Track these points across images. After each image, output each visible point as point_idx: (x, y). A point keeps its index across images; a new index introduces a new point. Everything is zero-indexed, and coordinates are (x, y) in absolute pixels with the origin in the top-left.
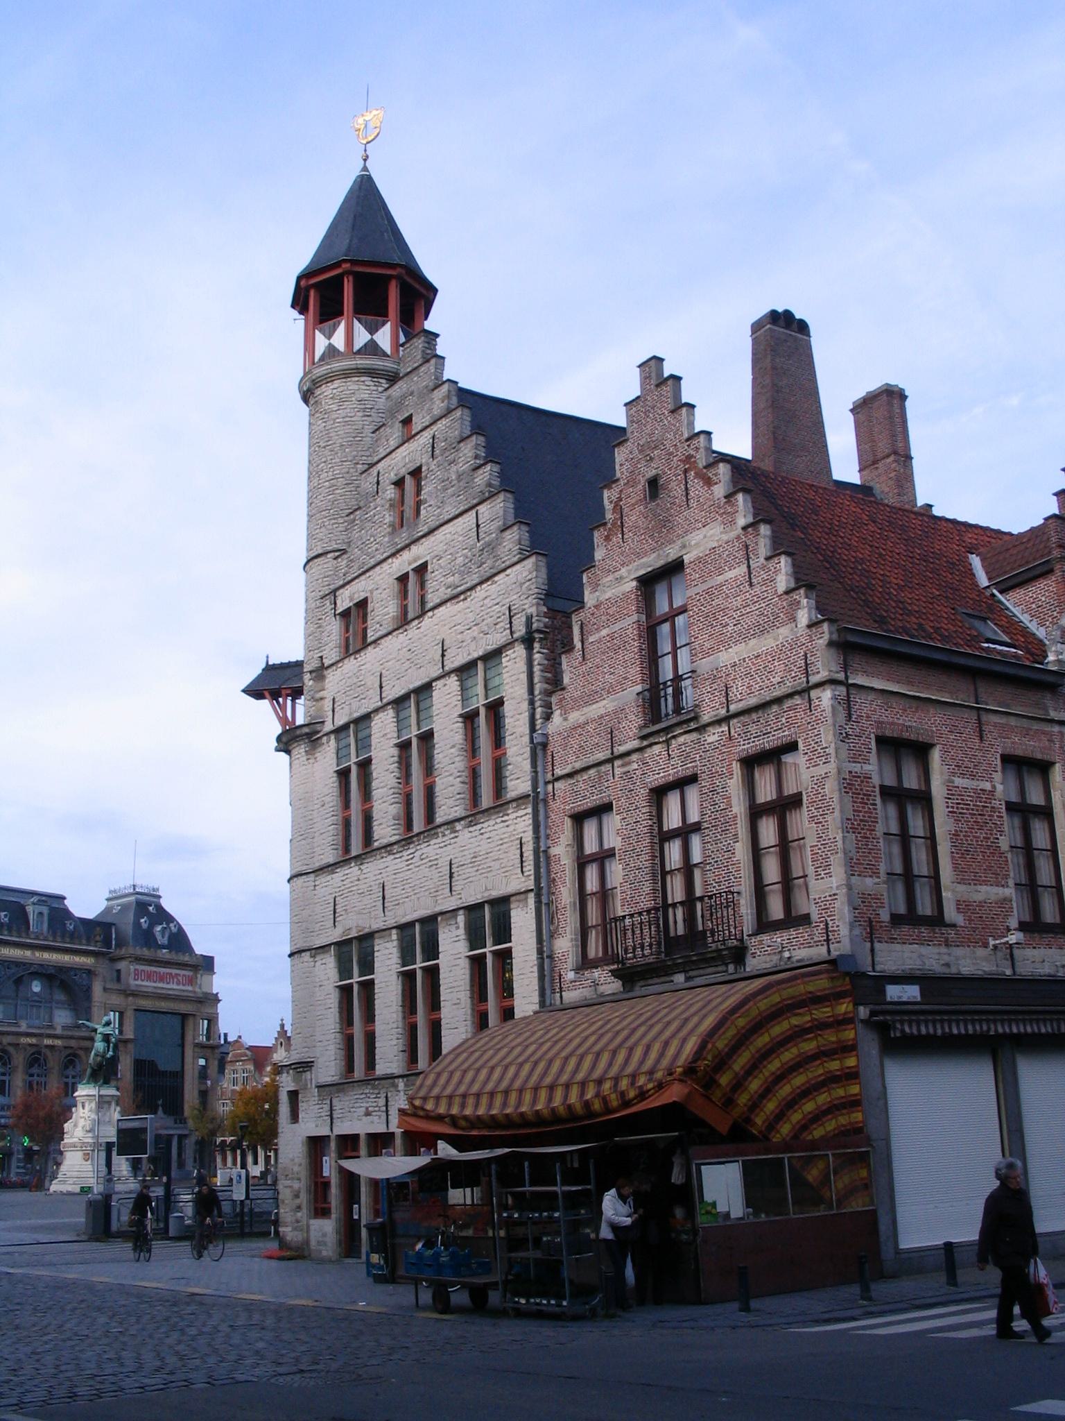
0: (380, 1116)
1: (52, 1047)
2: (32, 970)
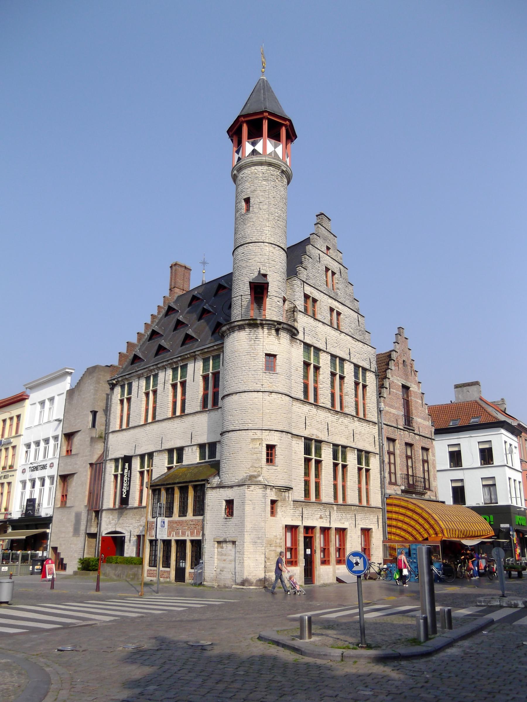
0: (326, 520)
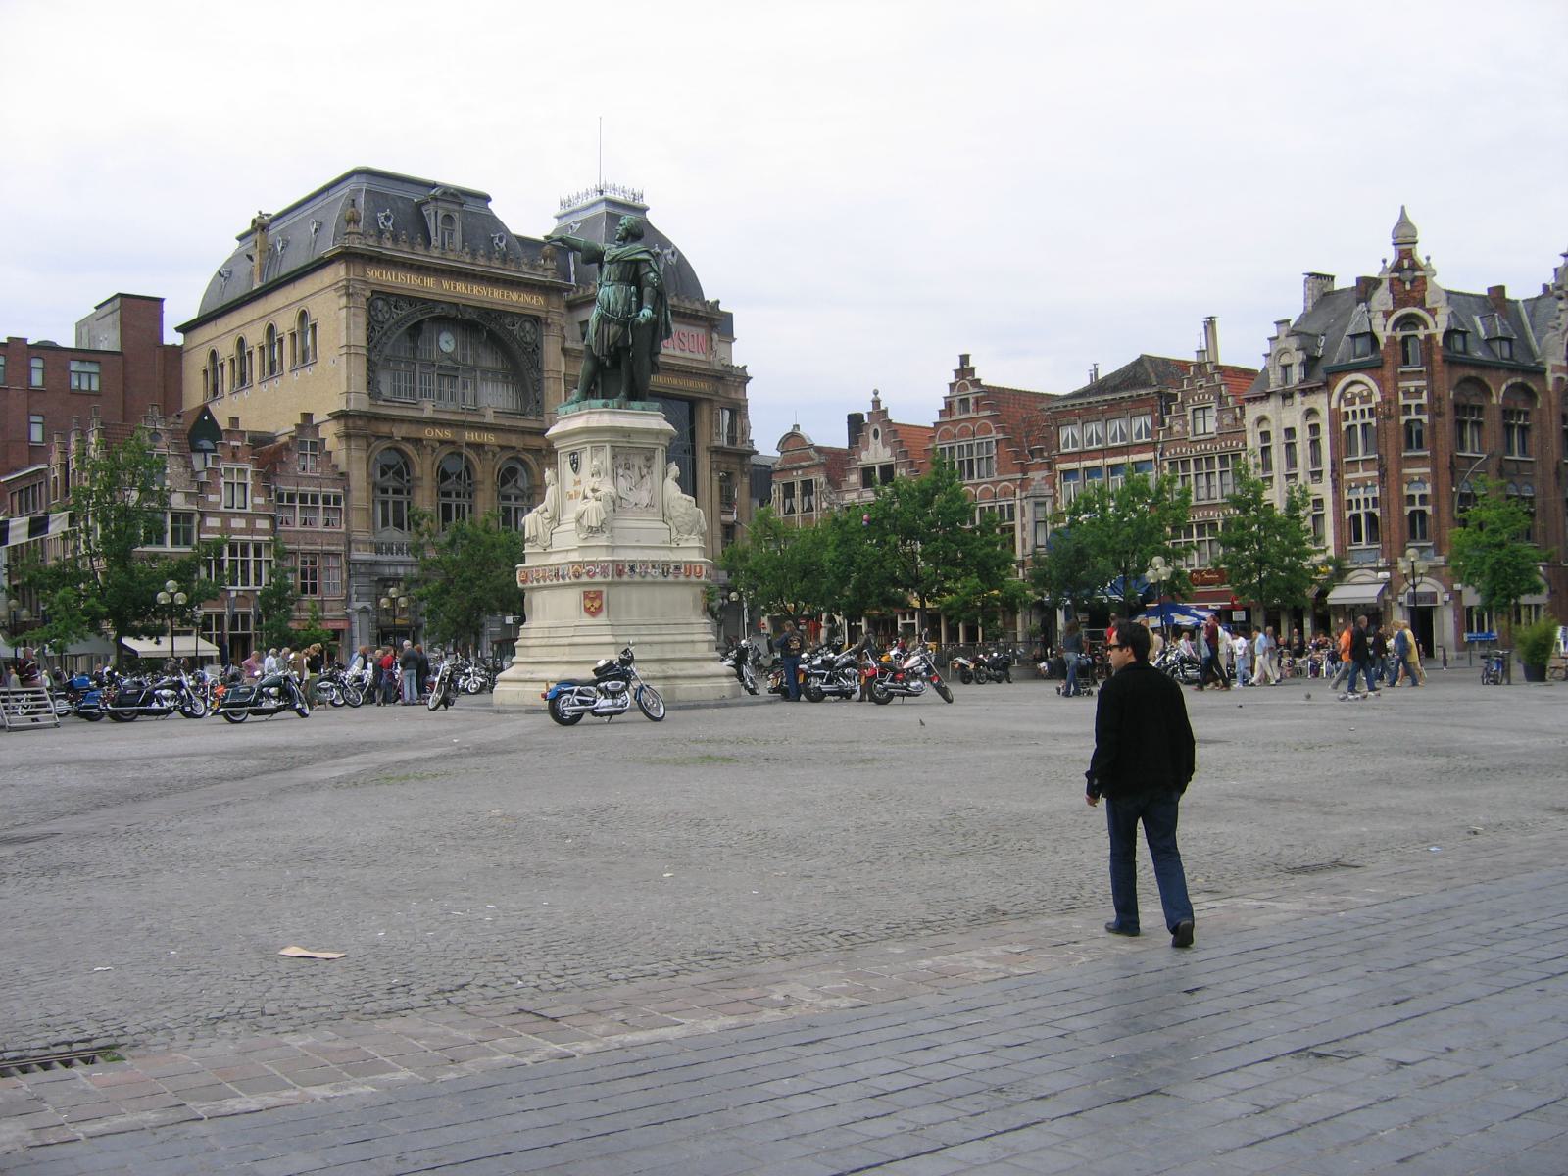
1: (478, 447)
2: (438, 311)
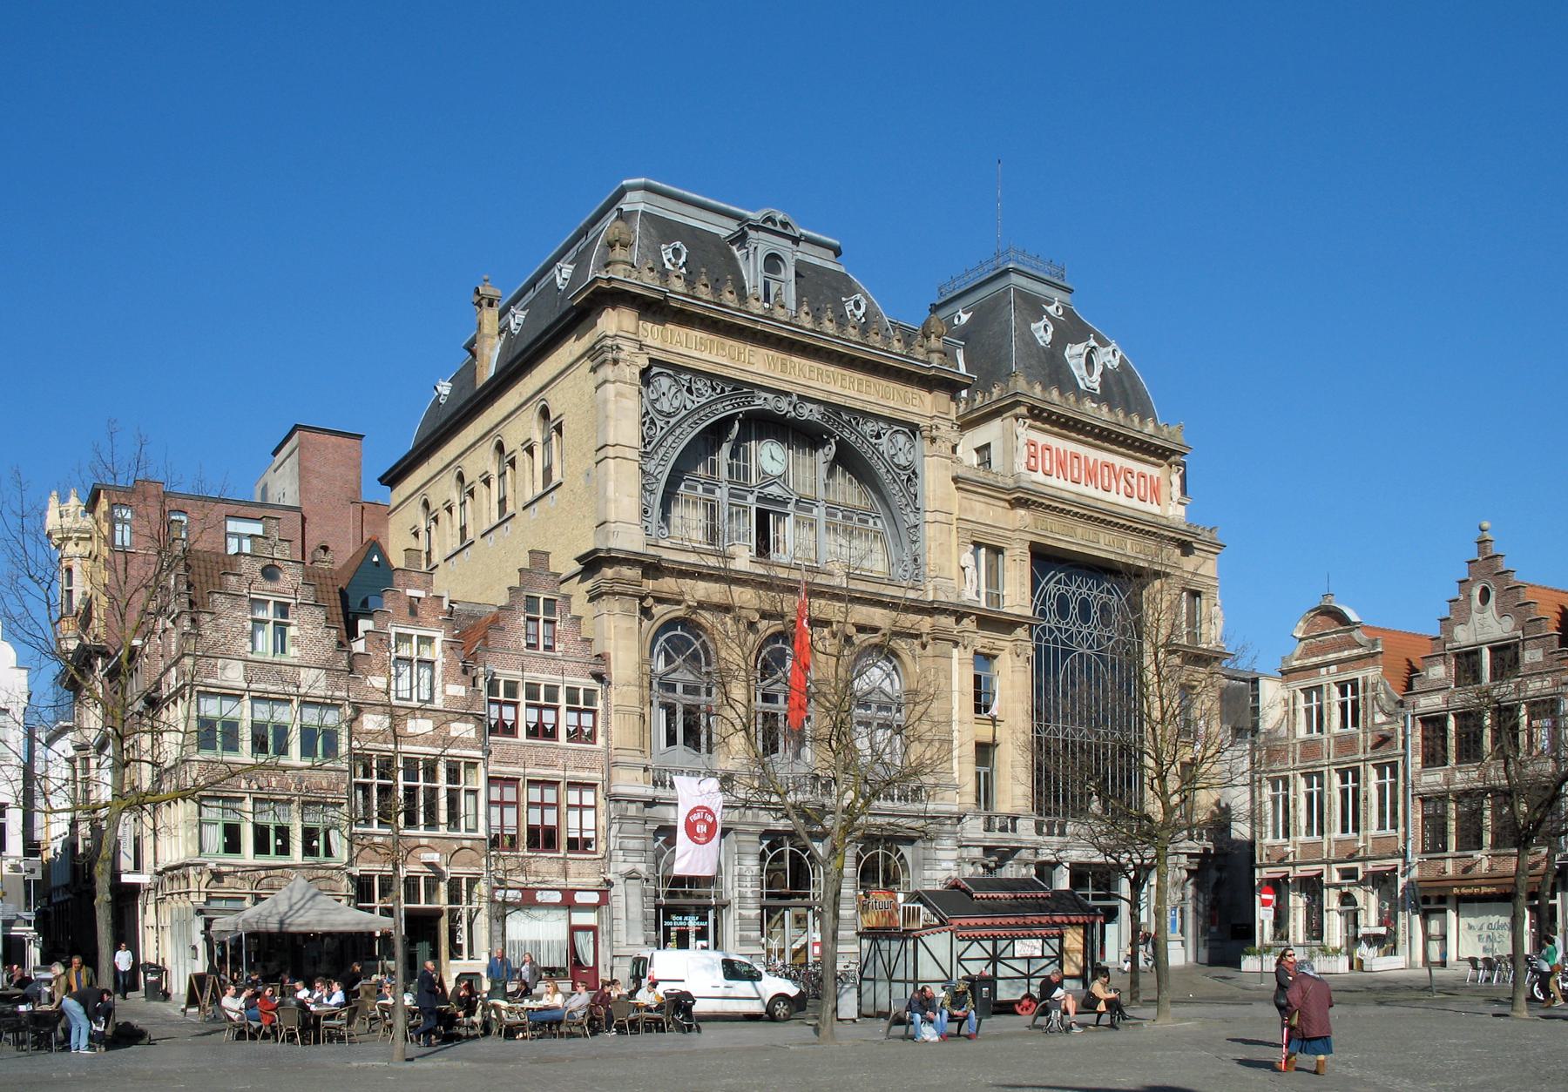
2: (762, 402)
